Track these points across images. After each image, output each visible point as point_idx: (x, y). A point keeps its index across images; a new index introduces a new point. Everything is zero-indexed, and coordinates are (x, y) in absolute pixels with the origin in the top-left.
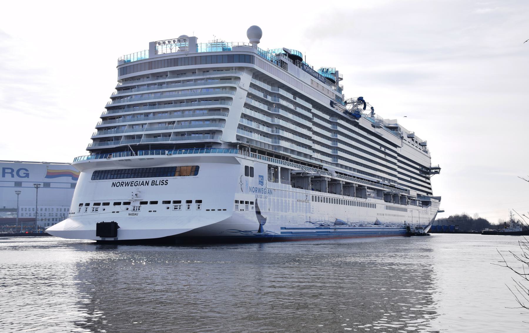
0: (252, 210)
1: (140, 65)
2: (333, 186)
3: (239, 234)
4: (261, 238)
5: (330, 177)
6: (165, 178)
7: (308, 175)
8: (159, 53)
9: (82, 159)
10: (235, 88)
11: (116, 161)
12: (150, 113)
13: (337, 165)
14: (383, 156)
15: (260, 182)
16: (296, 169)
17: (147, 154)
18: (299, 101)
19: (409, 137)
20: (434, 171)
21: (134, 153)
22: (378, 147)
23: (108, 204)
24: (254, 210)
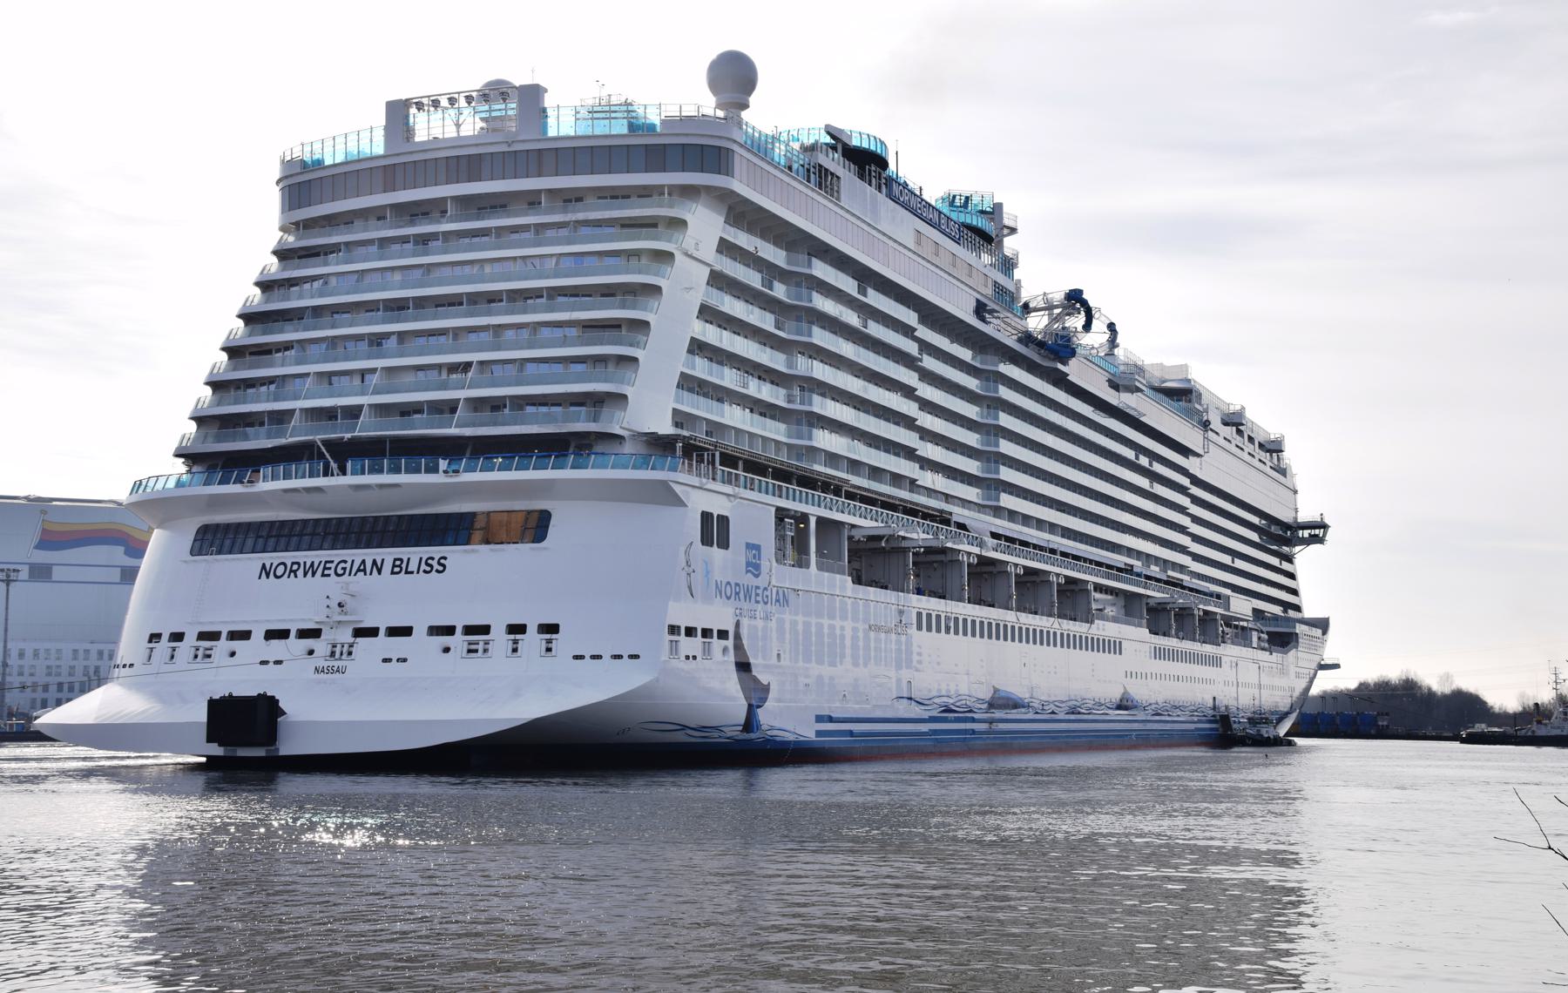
0: (722, 656)
1: (355, 174)
2: (985, 580)
3: (681, 737)
4: (752, 752)
5: (976, 550)
6: (436, 551)
7: (904, 544)
8: (417, 139)
9: (159, 486)
10: (671, 255)
11: (274, 493)
12: (387, 335)
13: (998, 511)
14: (1143, 482)
15: (748, 564)
16: (866, 522)
17: (372, 471)
18: (875, 299)
19: (1226, 424)
20: (1306, 533)
21: (333, 465)
22: (1129, 454)
23: (245, 635)
24: (731, 658)
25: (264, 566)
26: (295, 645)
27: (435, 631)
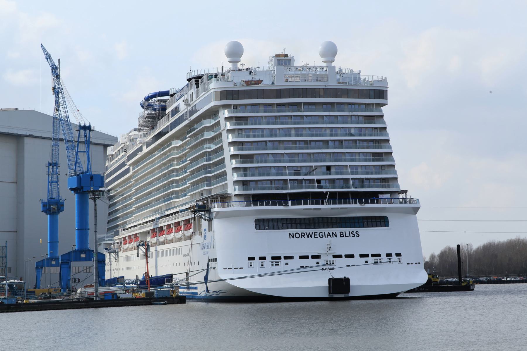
6: (355, 230)
23: (291, 258)
25: (290, 234)
27: (362, 256)
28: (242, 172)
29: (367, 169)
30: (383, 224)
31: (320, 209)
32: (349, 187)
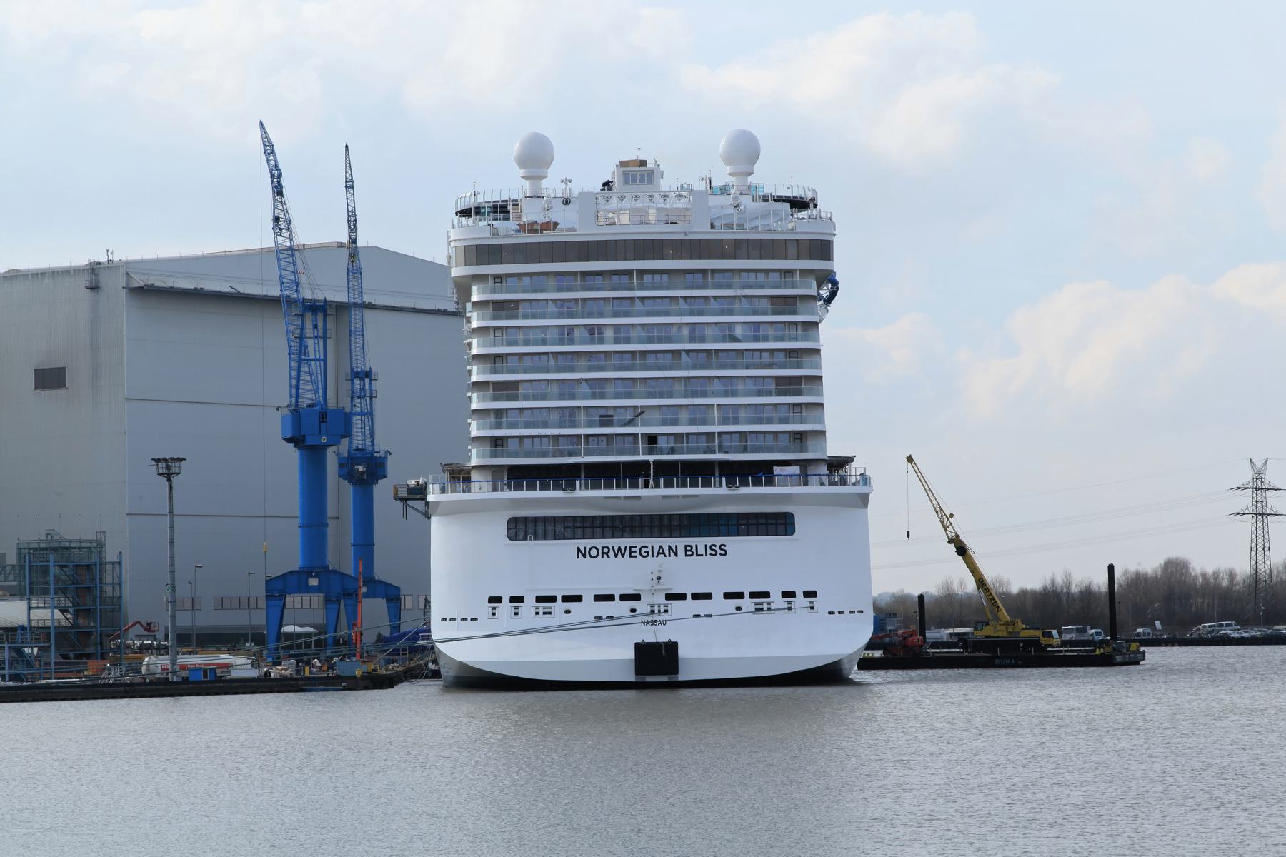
6: (718, 541)
11: (587, 498)
23: (578, 598)
25: (578, 549)
26: (619, 608)
27: (728, 596)
28: (492, 419)
29: (759, 413)
30: (781, 528)
31: (639, 498)
32: (713, 452)
